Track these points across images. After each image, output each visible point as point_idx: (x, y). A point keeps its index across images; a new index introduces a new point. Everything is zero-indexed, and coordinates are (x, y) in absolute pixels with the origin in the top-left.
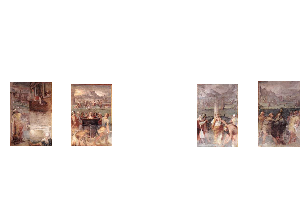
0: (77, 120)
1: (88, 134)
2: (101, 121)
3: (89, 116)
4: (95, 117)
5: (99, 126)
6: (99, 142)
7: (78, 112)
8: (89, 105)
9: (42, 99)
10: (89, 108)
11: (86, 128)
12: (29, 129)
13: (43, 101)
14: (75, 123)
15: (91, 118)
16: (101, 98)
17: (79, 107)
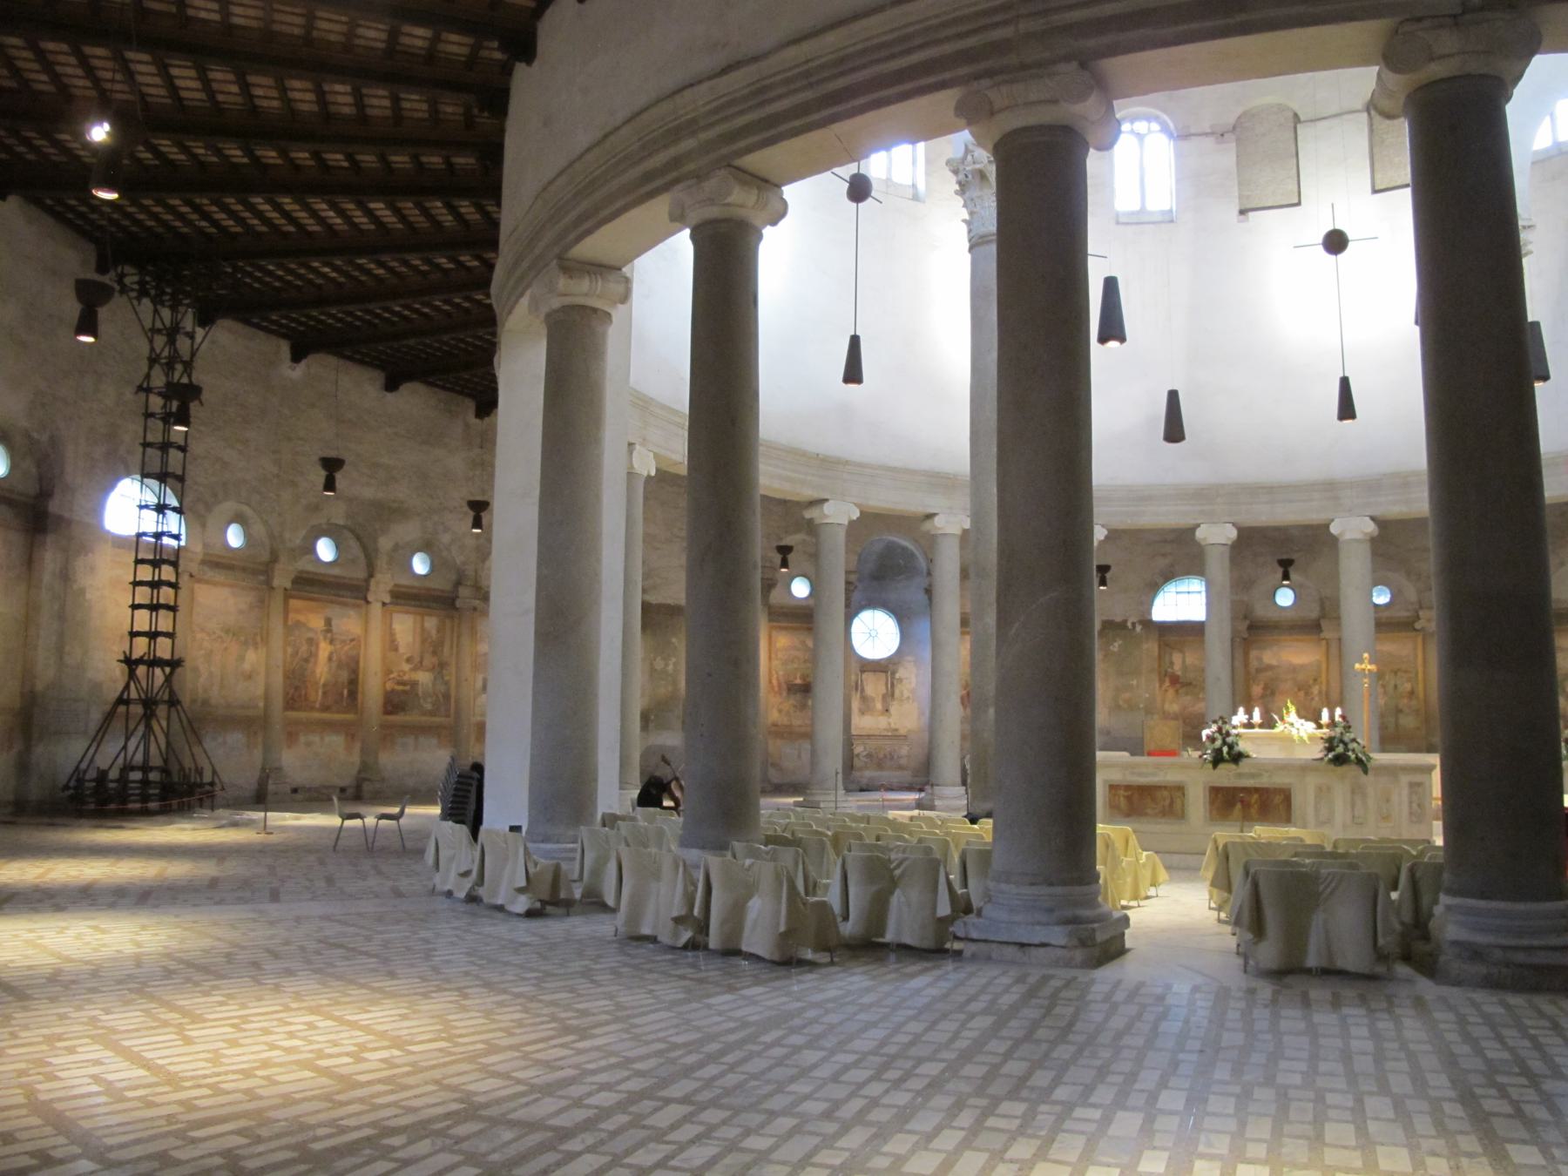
0: (780, 685)
1: (795, 706)
3: (796, 678)
4: (804, 680)
7: (781, 673)
10: (796, 666)
14: (776, 689)
15: (798, 681)
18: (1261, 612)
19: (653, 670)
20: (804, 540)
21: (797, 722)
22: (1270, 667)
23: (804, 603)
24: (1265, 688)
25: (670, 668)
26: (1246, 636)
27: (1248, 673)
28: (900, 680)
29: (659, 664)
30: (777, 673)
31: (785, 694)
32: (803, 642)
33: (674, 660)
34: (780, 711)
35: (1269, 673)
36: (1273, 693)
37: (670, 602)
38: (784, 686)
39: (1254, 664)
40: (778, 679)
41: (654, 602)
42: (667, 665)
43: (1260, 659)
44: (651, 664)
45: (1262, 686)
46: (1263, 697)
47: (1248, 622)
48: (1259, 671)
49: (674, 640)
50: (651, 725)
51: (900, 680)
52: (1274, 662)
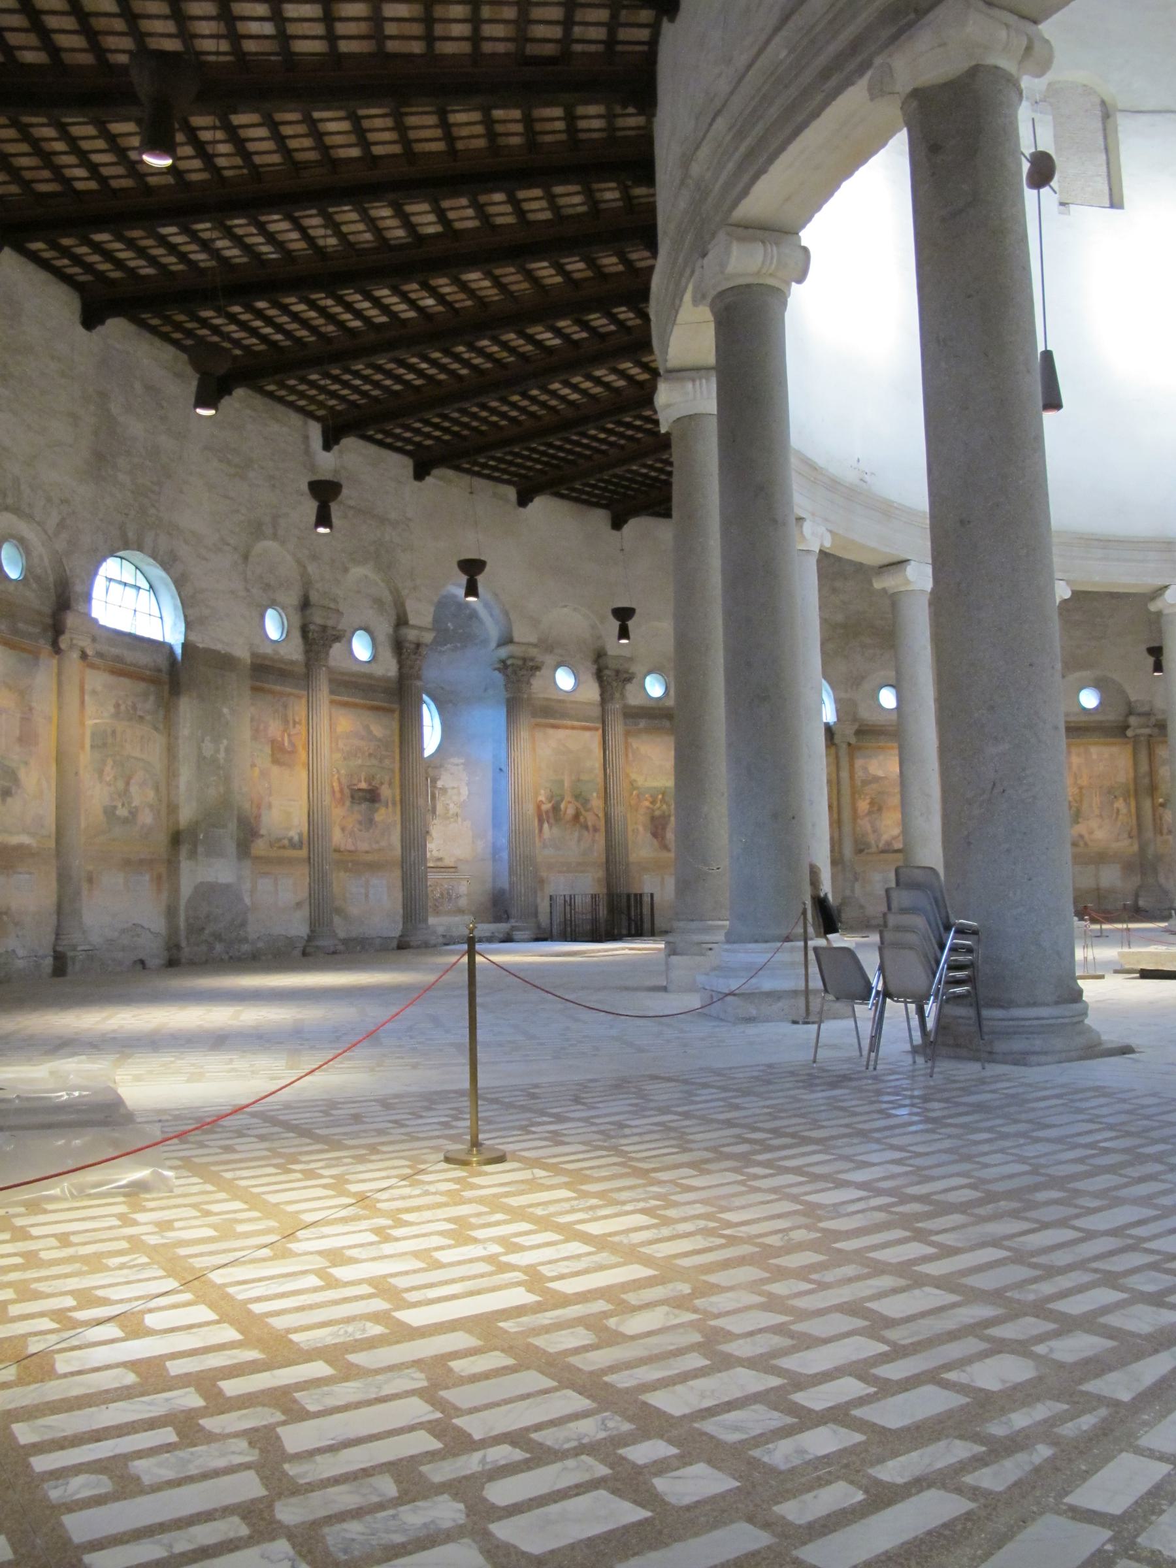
0: (341, 791)
1: (360, 823)
2: (379, 795)
3: (360, 781)
4: (370, 784)
5: (377, 805)
6: (377, 842)
7: (343, 772)
8: (359, 755)
9: (289, 735)
10: (359, 762)
11: (356, 808)
12: (270, 806)
13: (290, 741)
14: (338, 795)
15: (363, 785)
16: (380, 740)
17: (345, 759)
18: (865, 714)
19: (201, 758)
20: (366, 577)
21: (364, 846)
22: (876, 779)
23: (366, 669)
24: (872, 803)
25: (222, 755)
26: (853, 741)
27: (853, 786)
28: (444, 790)
29: (208, 748)
30: (338, 772)
31: (348, 803)
32: (367, 728)
33: (225, 742)
34: (343, 829)
35: (874, 786)
36: (880, 809)
37: (219, 647)
38: (347, 791)
39: (859, 774)
40: (339, 779)
41: (201, 646)
42: (217, 751)
43: (865, 769)
44: (200, 748)
45: (868, 801)
46: (870, 813)
47: (856, 727)
48: (865, 783)
49: (225, 710)
50: (200, 849)
51: (444, 790)
52: (880, 773)
